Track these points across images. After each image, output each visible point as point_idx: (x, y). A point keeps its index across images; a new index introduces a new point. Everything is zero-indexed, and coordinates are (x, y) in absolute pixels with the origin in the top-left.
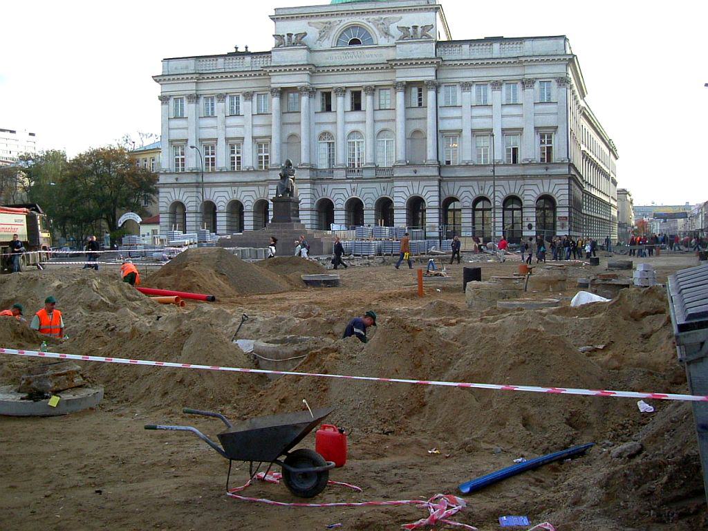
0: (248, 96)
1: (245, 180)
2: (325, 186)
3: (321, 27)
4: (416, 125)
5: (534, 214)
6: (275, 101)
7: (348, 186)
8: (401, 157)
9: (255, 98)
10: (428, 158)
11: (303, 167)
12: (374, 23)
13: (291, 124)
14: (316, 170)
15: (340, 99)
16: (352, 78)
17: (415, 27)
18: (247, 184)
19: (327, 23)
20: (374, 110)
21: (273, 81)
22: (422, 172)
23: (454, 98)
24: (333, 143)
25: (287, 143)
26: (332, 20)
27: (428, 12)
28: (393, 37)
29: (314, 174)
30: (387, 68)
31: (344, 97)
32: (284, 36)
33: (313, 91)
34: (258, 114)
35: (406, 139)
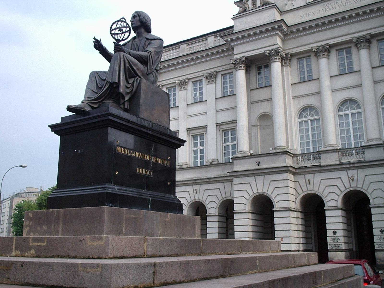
0: (211, 77)
1: (209, 177)
6: (241, 74)
7: (343, 175)
13: (261, 101)
15: (323, 62)
16: (337, 32)
18: (209, 181)
20: (373, 68)
24: (318, 120)
29: (293, 162)
31: (328, 59)
34: (222, 97)
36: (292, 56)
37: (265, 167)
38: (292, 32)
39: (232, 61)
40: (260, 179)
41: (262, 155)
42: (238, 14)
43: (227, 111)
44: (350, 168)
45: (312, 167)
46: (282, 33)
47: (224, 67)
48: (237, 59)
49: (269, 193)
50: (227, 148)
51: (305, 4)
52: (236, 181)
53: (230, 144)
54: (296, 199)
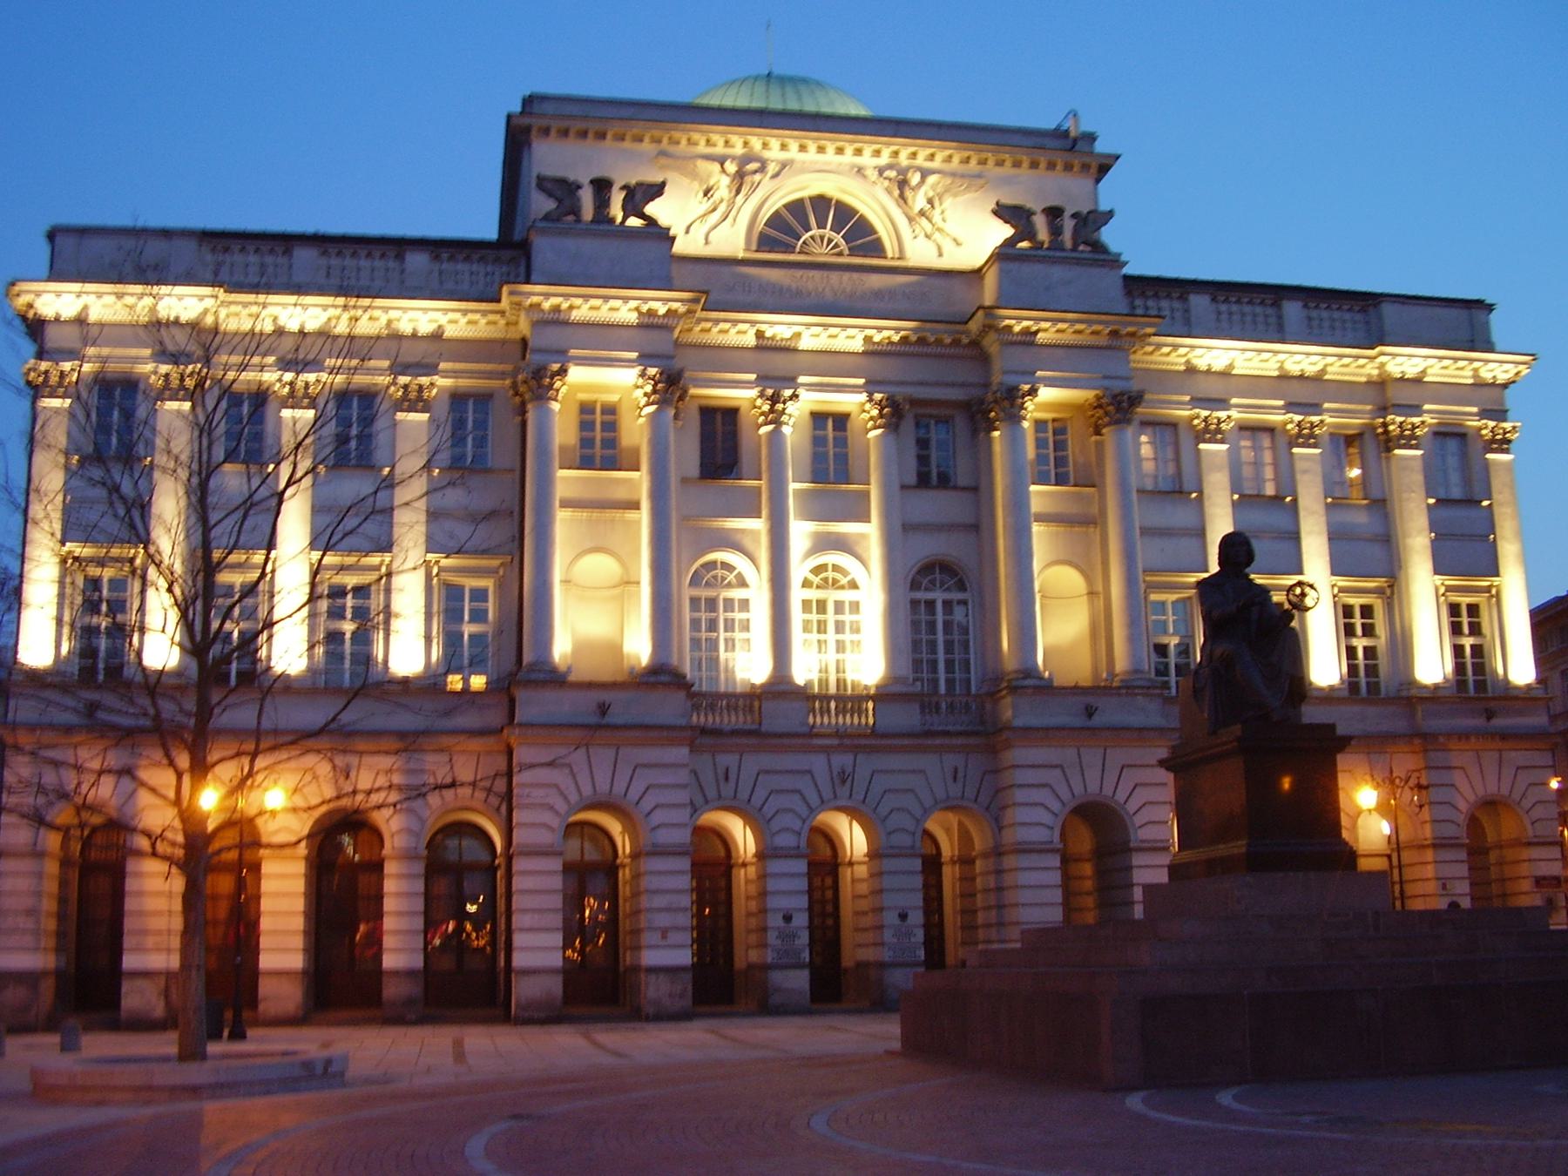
2: (728, 760)
5: (1463, 870)
37: (620, 721)
40: (603, 756)
44: (841, 748)
45: (735, 733)
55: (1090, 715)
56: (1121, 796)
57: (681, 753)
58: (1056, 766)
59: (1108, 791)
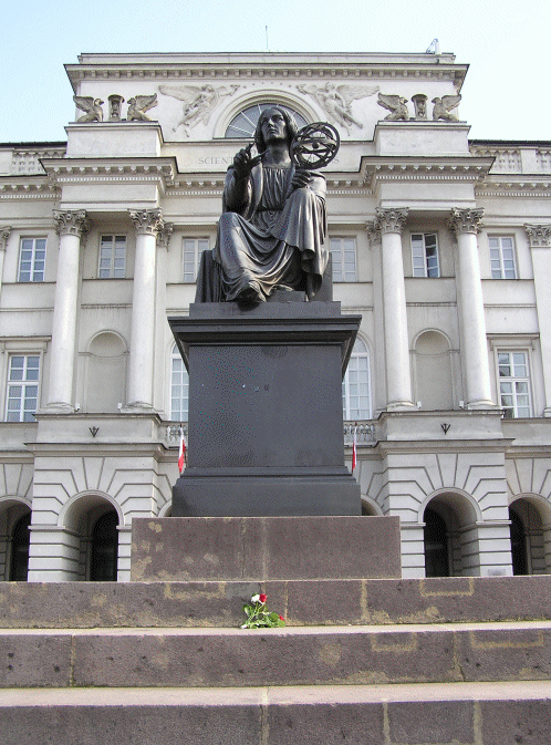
3: (191, 98)
4: (431, 319)
6: (71, 243)
8: (404, 390)
9: (15, 243)
10: (472, 396)
11: (137, 411)
12: (314, 96)
13: (104, 306)
14: (167, 423)
17: (419, 99)
19: (204, 89)
21: (66, 195)
22: (462, 430)
23: (512, 263)
25: (90, 354)
26: (215, 84)
27: (439, 80)
28: (361, 127)
30: (354, 184)
32: (101, 103)
33: (167, 232)
35: (411, 351)
36: (177, 229)
38: (182, 185)
39: (57, 214)
40: (94, 464)
41: (104, 416)
42: (79, 122)
43: (24, 315)
46: (165, 182)
47: (30, 222)
48: (69, 212)
49: (112, 493)
50: (15, 391)
51: (210, 139)
52: (40, 462)
53: (24, 383)
54: (159, 509)
55: (445, 431)
56: (469, 489)
57: (149, 462)
58: (421, 467)
59: (460, 485)
